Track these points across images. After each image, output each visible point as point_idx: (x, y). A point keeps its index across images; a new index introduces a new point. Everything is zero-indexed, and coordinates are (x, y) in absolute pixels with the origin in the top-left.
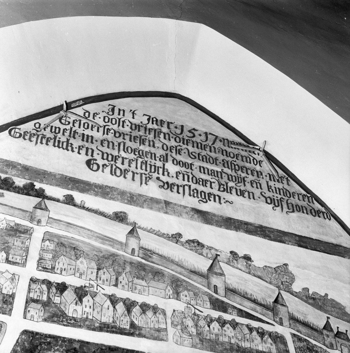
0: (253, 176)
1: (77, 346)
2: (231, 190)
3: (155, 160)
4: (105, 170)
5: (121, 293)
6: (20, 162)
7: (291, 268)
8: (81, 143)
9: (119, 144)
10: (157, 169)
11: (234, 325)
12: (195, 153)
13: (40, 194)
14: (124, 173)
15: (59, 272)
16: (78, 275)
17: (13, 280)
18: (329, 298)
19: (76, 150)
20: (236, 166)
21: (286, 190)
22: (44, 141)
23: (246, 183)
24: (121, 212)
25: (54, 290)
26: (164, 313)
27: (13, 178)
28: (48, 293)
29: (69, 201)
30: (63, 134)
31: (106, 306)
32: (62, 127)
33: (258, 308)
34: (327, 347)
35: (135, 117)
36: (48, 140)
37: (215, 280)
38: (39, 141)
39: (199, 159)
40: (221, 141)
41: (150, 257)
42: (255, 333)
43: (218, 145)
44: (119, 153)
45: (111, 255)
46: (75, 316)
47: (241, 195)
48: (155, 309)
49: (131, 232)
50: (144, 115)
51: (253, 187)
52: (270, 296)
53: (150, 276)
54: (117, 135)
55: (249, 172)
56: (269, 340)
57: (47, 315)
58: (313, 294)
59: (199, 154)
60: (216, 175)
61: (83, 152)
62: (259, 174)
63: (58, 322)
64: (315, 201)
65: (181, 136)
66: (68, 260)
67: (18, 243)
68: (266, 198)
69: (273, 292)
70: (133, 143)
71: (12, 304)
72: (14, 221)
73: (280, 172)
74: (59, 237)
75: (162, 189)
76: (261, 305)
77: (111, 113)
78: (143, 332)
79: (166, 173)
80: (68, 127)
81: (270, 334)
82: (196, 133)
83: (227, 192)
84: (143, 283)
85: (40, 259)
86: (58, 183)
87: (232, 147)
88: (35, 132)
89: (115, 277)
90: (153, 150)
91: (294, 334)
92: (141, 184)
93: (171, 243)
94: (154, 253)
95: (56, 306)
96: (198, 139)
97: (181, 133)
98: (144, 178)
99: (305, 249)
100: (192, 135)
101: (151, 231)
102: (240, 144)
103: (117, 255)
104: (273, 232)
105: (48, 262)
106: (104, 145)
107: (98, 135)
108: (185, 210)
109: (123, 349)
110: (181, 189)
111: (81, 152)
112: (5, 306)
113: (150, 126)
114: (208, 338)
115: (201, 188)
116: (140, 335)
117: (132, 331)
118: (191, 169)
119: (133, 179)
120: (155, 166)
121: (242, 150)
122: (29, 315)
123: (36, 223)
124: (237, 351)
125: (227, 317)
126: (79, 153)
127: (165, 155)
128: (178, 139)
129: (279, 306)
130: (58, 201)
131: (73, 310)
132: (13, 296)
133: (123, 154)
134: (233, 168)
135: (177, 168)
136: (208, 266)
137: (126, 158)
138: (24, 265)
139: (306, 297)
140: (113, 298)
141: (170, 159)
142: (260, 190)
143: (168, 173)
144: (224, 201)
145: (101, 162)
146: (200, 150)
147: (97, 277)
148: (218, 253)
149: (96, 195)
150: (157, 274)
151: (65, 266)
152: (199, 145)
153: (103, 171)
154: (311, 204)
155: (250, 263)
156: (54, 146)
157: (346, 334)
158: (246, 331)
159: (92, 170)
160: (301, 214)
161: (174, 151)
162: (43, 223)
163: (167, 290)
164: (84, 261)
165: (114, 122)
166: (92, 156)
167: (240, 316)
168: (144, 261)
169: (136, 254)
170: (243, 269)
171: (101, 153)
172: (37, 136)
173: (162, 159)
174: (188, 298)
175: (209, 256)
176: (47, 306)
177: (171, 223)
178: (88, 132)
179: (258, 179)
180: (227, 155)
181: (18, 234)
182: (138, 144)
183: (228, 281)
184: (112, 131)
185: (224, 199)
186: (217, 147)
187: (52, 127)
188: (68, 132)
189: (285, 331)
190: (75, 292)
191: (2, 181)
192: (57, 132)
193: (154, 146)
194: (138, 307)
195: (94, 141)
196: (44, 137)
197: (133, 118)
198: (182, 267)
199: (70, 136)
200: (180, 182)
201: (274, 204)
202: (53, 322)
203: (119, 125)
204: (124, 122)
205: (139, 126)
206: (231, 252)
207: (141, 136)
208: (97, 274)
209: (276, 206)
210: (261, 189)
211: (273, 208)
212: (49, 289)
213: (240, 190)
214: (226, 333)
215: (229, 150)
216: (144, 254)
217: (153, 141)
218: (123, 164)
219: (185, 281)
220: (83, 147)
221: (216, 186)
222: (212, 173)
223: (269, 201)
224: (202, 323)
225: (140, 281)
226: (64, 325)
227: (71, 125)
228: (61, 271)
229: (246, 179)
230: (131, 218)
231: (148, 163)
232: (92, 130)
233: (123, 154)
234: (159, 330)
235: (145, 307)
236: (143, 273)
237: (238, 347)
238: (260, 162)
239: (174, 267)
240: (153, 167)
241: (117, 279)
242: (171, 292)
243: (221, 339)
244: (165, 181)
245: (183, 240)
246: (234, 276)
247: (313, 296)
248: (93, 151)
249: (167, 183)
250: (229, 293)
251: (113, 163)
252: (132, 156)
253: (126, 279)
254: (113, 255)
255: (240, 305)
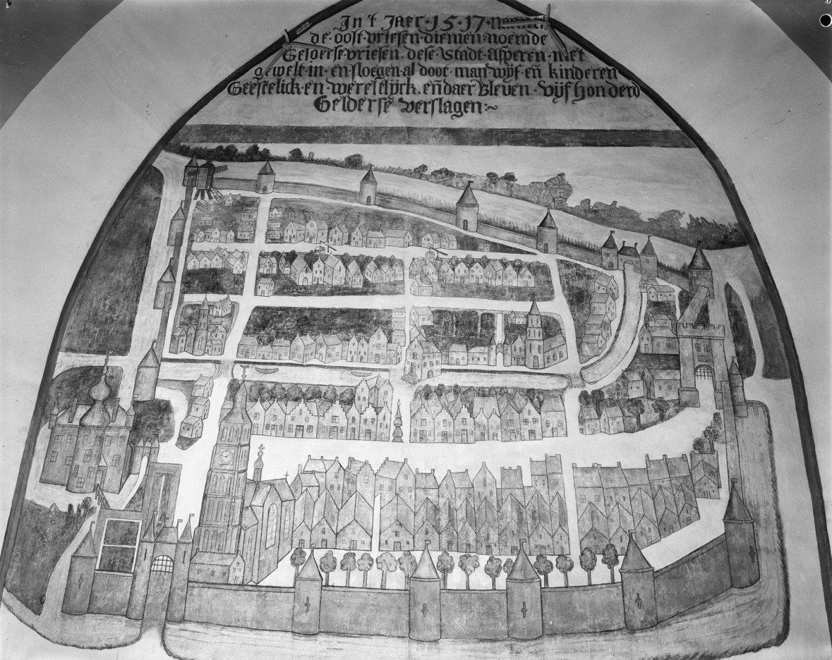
0: (530, 61)
1: (307, 314)
2: (496, 90)
3: (398, 76)
4: (336, 107)
5: (353, 251)
6: (242, 123)
7: (567, 178)
8: (307, 80)
9: (354, 68)
10: (399, 87)
11: (485, 262)
12: (451, 50)
13: (266, 157)
14: (358, 105)
15: (288, 240)
16: (308, 239)
17: (242, 258)
18: (617, 206)
19: (303, 91)
20: (508, 54)
21: (577, 69)
22: (267, 90)
23: (519, 74)
24: (355, 156)
25: (283, 260)
26: (402, 263)
27: (235, 144)
28: (278, 265)
29: (297, 156)
30: (288, 74)
31: (337, 268)
32: (286, 65)
33: (518, 237)
34: (604, 268)
35: (375, 23)
36: (270, 88)
37: (466, 214)
38: (261, 91)
39: (456, 58)
40: (488, 23)
41: (388, 202)
42: (510, 267)
43: (486, 29)
44: (353, 79)
45: (343, 210)
46: (305, 284)
47: (509, 93)
48: (391, 262)
49: (366, 178)
50: (386, 17)
51: (528, 77)
52: (535, 220)
53: (387, 224)
54: (351, 56)
55: (525, 57)
56: (528, 273)
57: (277, 288)
58: (594, 206)
59: (456, 51)
60: (477, 74)
61: (311, 91)
62: (541, 56)
63: (289, 294)
64: (618, 75)
65: (433, 33)
66: (296, 225)
67: (246, 219)
68: (545, 89)
69: (540, 212)
70: (371, 60)
71: (243, 283)
72: (240, 195)
73: (570, 44)
74: (286, 201)
75: (406, 113)
76: (521, 233)
77: (344, 28)
78: (377, 288)
79: (411, 90)
80: (293, 63)
81: (529, 267)
82: (454, 22)
83: (491, 94)
84: (380, 234)
85: (268, 230)
86: (283, 138)
87: (504, 28)
88: (255, 81)
89: (347, 234)
90: (395, 63)
91: (561, 261)
92: (379, 113)
93: (412, 179)
94: (393, 196)
95: (286, 278)
96: (456, 31)
97: (435, 28)
98: (383, 105)
99: (592, 148)
100: (449, 26)
101: (390, 171)
102: (516, 20)
103: (350, 208)
104: (548, 134)
105: (277, 232)
106: (335, 74)
107: (327, 63)
108: (433, 134)
109: (356, 310)
110: (429, 107)
111: (308, 91)
112: (236, 286)
113: (393, 30)
114: (452, 282)
115: (455, 98)
116: (374, 293)
117: (366, 289)
118: (445, 75)
119: (370, 110)
120: (397, 85)
121: (519, 27)
122: (259, 292)
123: (261, 192)
124: (485, 291)
125: (476, 255)
126: (306, 93)
127: (410, 66)
128: (429, 39)
129: (546, 230)
130: (284, 159)
131: (303, 278)
132: (243, 275)
133: (358, 80)
134: (503, 57)
135: (426, 79)
136: (458, 198)
137: (362, 84)
138: (252, 240)
139: (585, 211)
140: (345, 258)
141: (417, 68)
142: (538, 79)
143: (414, 89)
144: (486, 107)
145: (331, 98)
146: (459, 45)
147: (328, 238)
148: (472, 179)
149: (326, 142)
150: (396, 221)
151: (295, 233)
152: (458, 37)
153: (334, 109)
154: (613, 81)
155: (512, 182)
156: (278, 92)
157: (635, 248)
158: (499, 266)
159: (321, 111)
160: (595, 99)
161: (423, 57)
162: (269, 190)
163: (406, 238)
164: (315, 223)
165: (347, 39)
166: (321, 93)
167: (494, 251)
168: (381, 209)
169: (372, 202)
170: (503, 192)
171: (331, 86)
172: (262, 88)
173: (406, 73)
174: (431, 242)
175: (460, 185)
176: (276, 279)
177: (414, 155)
178: (317, 63)
179: (537, 64)
180: (495, 42)
181: (245, 208)
182: (377, 60)
183: (482, 212)
184: (345, 52)
185: (486, 105)
186: (482, 34)
187: (275, 68)
188: (293, 69)
189: (550, 260)
190: (305, 259)
191: (224, 151)
192: (281, 73)
193: (397, 58)
194: (372, 263)
195: (323, 73)
196: (266, 83)
197: (372, 26)
198: (427, 207)
199: (295, 75)
200: (429, 97)
201: (556, 95)
202: (284, 294)
203: (354, 42)
204: (359, 35)
205: (379, 34)
206: (488, 175)
207: (381, 49)
208: (328, 234)
209: (558, 97)
210: (540, 77)
211: (553, 101)
212: (278, 261)
213: (509, 86)
214: (474, 274)
215: (498, 32)
216: (382, 200)
217: (396, 51)
218: (357, 93)
219: (428, 222)
220: (310, 84)
221: (475, 90)
222: (473, 73)
223: (549, 92)
224: (445, 267)
225: (376, 233)
226: (295, 295)
227: (297, 59)
228: (290, 239)
229: (519, 69)
230: (367, 160)
231: (389, 82)
232: (321, 58)
233: (358, 80)
234: (394, 284)
235: (380, 262)
236: (379, 223)
237: (487, 287)
238: (542, 39)
239: (416, 208)
240: (395, 87)
241: (350, 236)
242: (411, 238)
243: (467, 281)
244: (409, 101)
245: (428, 172)
246: (489, 204)
247: (595, 208)
248: (322, 85)
249: (412, 103)
250: (481, 226)
251: (345, 95)
252: (369, 79)
253: (359, 234)
254: (346, 209)
255: (495, 237)
